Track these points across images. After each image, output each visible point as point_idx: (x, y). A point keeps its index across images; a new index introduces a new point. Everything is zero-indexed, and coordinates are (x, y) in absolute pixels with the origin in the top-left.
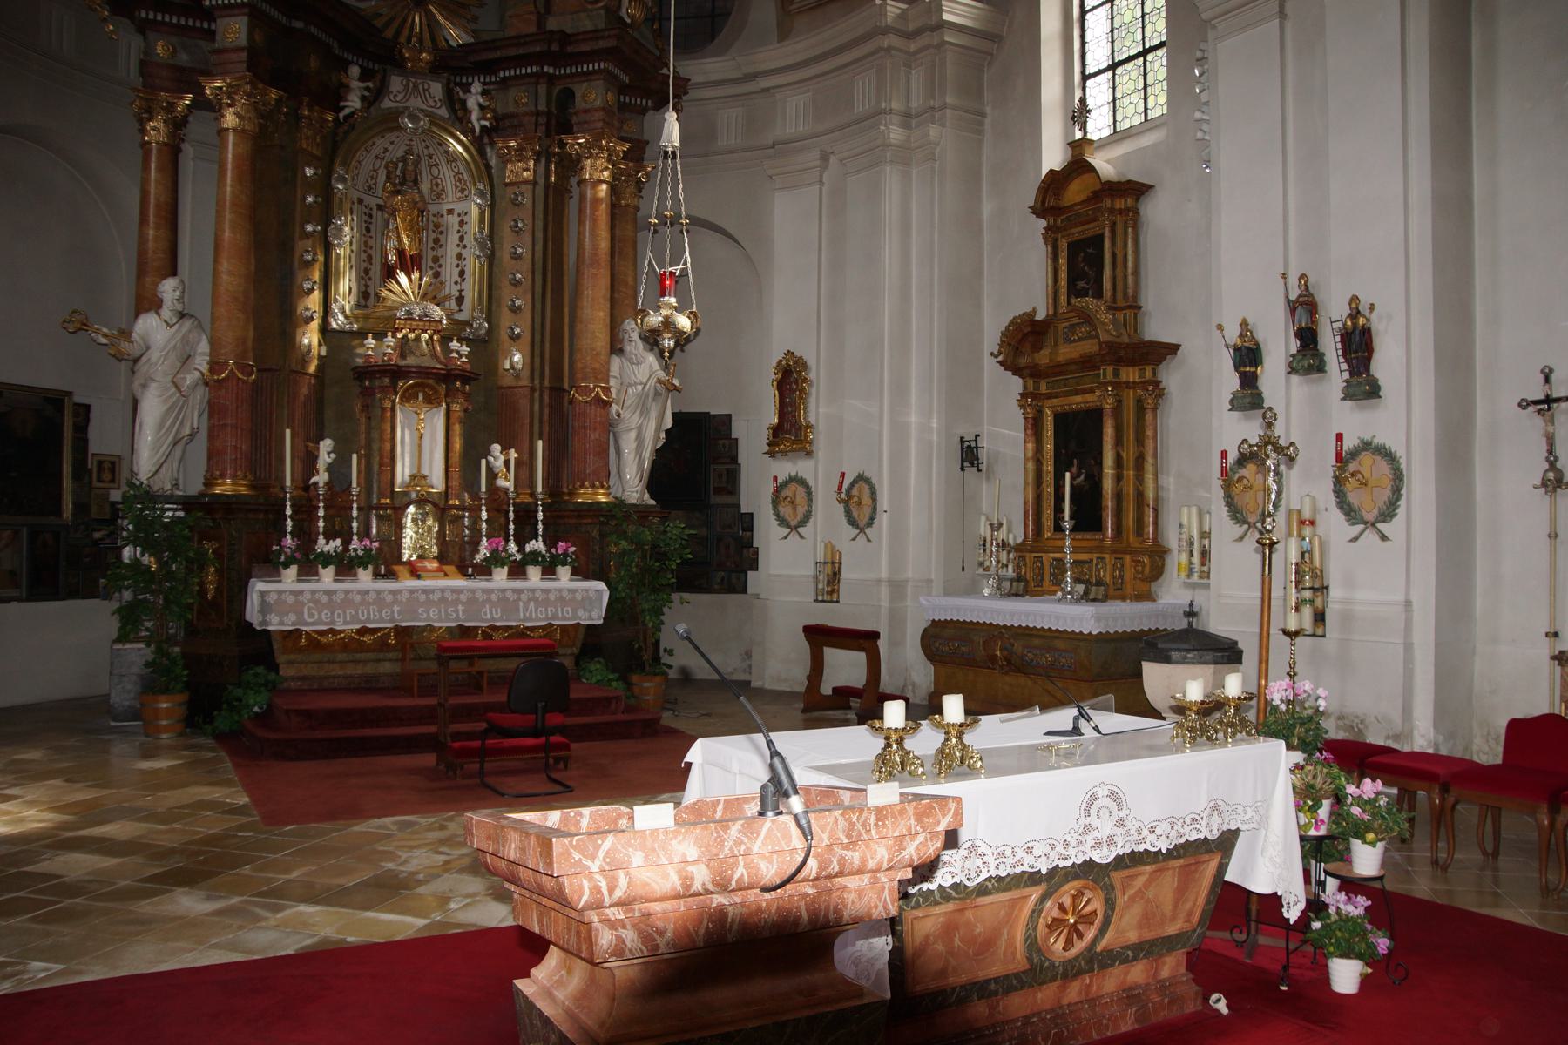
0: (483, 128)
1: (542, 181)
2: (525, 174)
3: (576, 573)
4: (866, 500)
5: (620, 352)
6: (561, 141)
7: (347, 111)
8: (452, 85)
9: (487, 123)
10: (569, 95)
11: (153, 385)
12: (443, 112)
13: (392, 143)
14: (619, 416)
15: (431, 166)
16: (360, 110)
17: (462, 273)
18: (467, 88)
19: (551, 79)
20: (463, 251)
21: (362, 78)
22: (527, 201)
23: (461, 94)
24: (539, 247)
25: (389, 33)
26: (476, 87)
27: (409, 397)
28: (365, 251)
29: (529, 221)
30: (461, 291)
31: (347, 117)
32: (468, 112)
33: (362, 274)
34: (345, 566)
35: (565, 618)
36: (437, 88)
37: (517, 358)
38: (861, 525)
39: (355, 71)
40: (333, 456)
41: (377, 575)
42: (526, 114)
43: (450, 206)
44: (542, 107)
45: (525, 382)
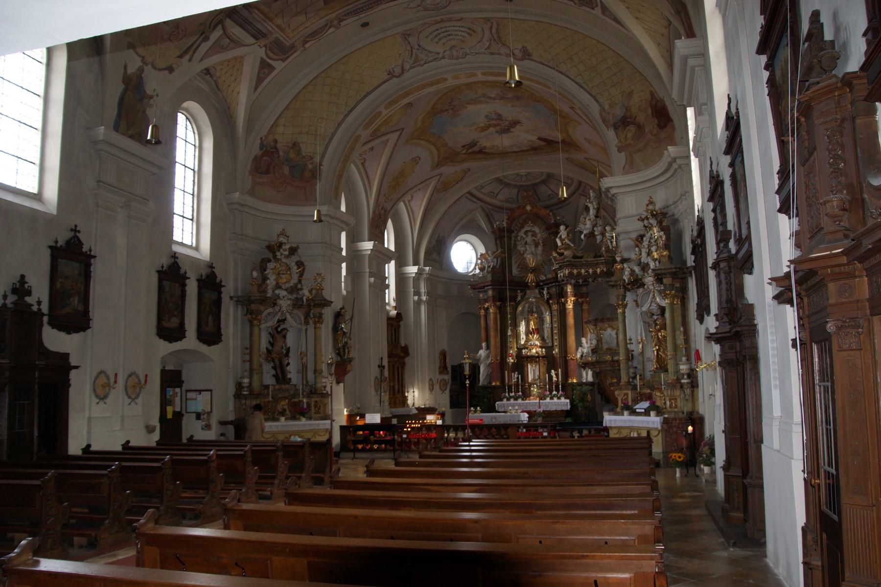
3: (565, 398)
5: (581, 346)
10: (562, 288)
12: (539, 296)
18: (543, 290)
19: (559, 285)
21: (521, 292)
22: (556, 314)
26: (546, 289)
27: (531, 362)
34: (516, 399)
35: (559, 409)
36: (537, 291)
37: (557, 350)
39: (519, 291)
41: (523, 400)
45: (558, 356)
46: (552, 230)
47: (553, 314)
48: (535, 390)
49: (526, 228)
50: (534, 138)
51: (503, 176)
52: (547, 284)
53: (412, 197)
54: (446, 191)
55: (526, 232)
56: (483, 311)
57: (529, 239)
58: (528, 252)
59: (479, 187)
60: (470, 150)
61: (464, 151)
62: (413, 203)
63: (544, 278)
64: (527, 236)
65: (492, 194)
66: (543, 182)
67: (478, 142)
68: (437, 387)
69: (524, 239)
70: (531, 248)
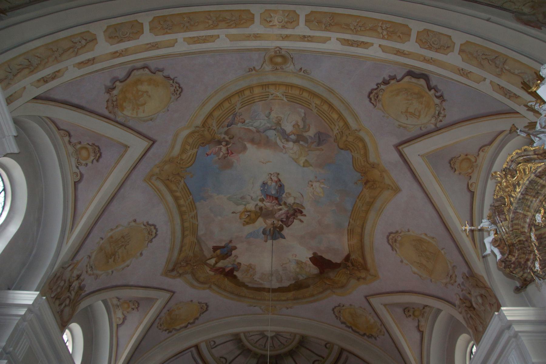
50: (305, 255)
51: (244, 333)
53: (125, 319)
54: (170, 332)
59: (212, 343)
60: (220, 264)
61: (212, 261)
62: (123, 331)
67: (235, 248)
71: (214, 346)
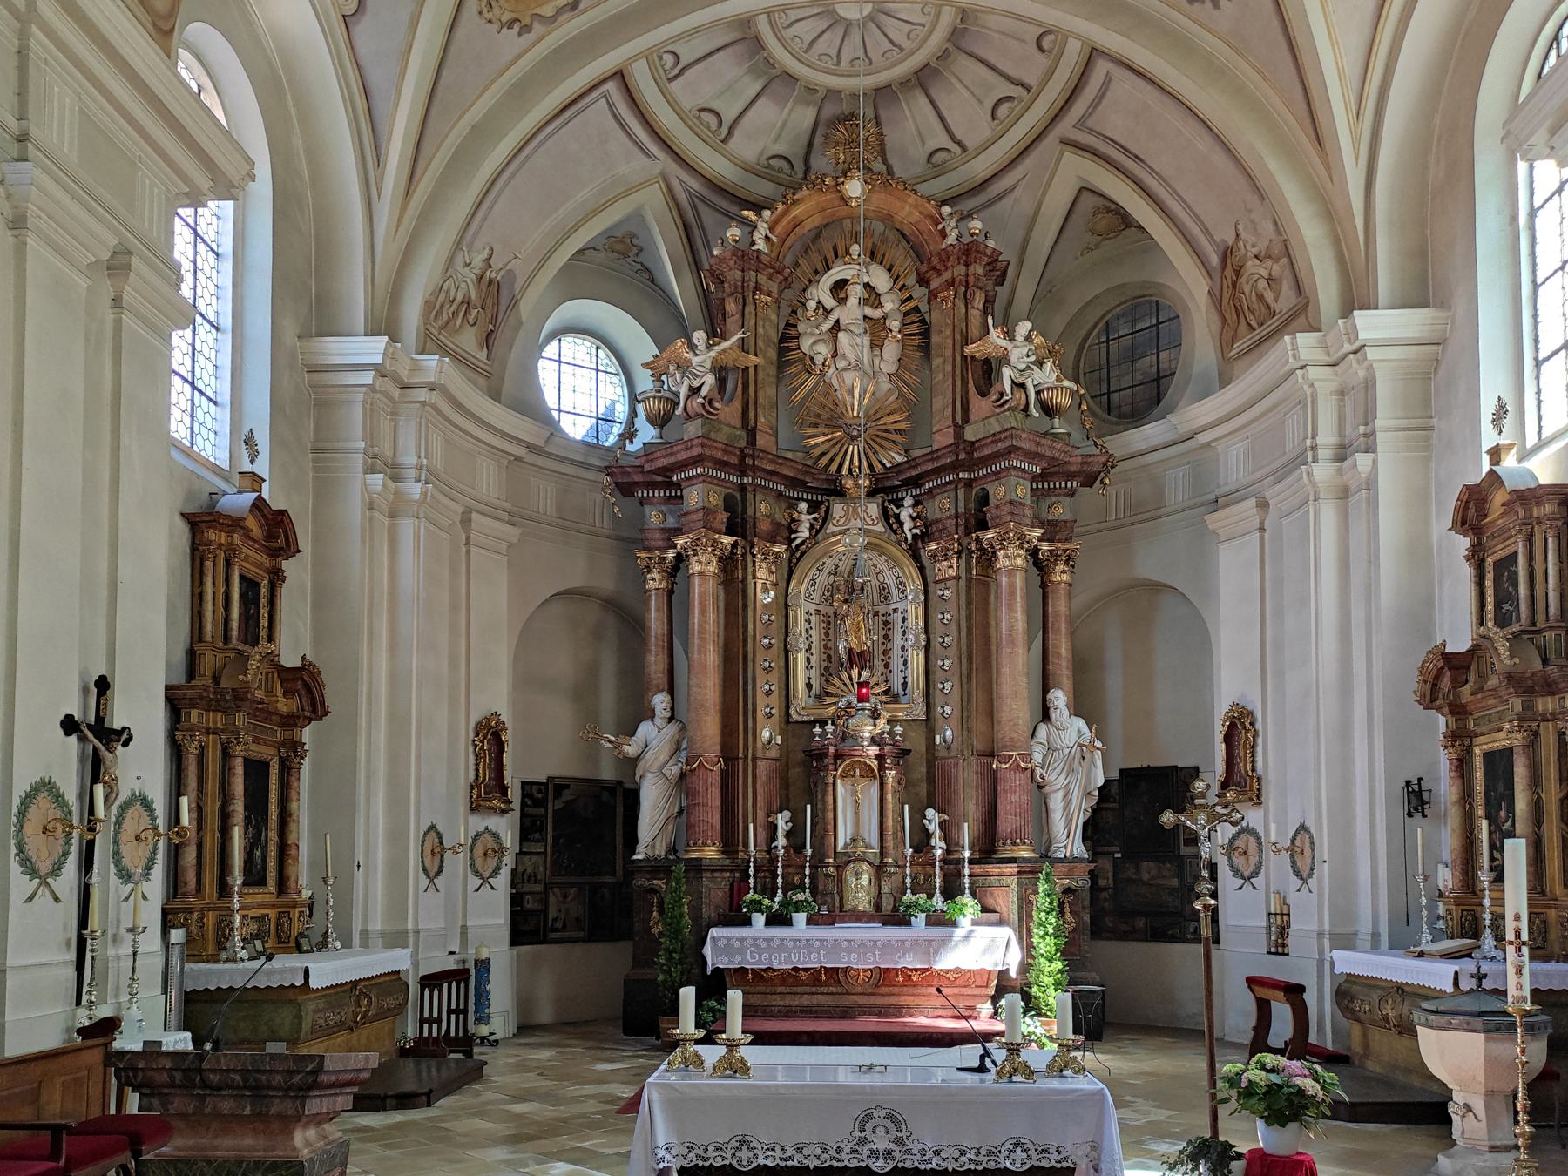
0: (914, 536)
1: (963, 576)
2: (950, 571)
4: (1307, 851)
6: (978, 537)
7: (798, 541)
8: (886, 504)
9: (917, 531)
11: (649, 776)
12: (880, 528)
13: (841, 560)
14: (1043, 778)
15: (877, 574)
16: (809, 538)
17: (905, 663)
18: (899, 503)
19: (969, 484)
20: (906, 644)
21: (809, 513)
23: (895, 509)
24: (964, 634)
25: (834, 468)
26: (908, 501)
28: (824, 653)
29: (954, 612)
30: (905, 678)
31: (798, 546)
32: (901, 524)
33: (823, 672)
36: (873, 508)
37: (948, 733)
38: (1305, 876)
40: (790, 824)
42: (947, 518)
43: (894, 606)
44: (961, 510)
46: (947, 275)
47: (933, 600)
48: (860, 889)
49: (838, 272)
52: (915, 482)
55: (840, 286)
56: (657, 577)
57: (852, 312)
58: (841, 364)
63: (899, 459)
64: (842, 301)
65: (711, 119)
66: (923, 79)
68: (456, 864)
69: (827, 312)
70: (853, 344)
71: (676, 71)
